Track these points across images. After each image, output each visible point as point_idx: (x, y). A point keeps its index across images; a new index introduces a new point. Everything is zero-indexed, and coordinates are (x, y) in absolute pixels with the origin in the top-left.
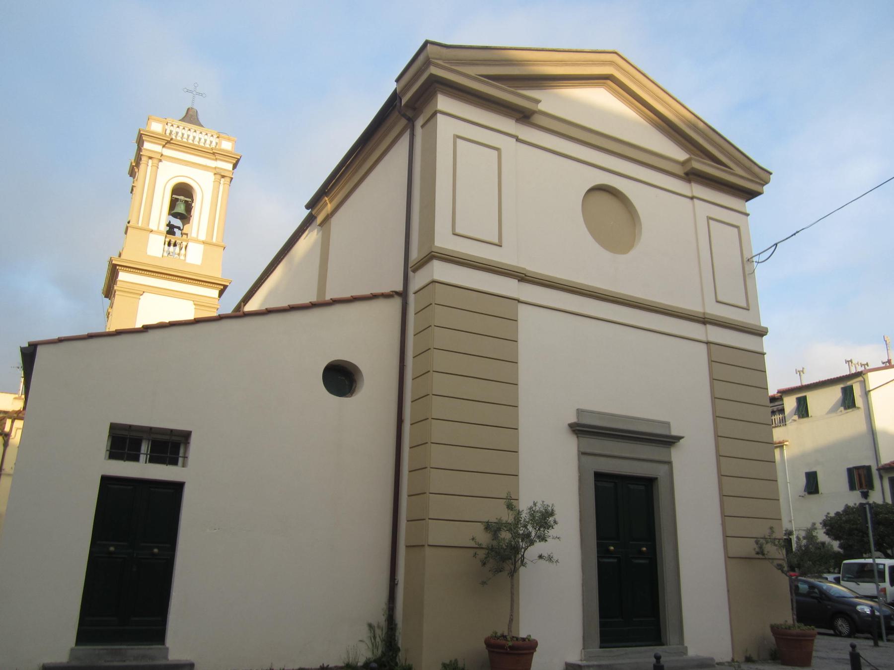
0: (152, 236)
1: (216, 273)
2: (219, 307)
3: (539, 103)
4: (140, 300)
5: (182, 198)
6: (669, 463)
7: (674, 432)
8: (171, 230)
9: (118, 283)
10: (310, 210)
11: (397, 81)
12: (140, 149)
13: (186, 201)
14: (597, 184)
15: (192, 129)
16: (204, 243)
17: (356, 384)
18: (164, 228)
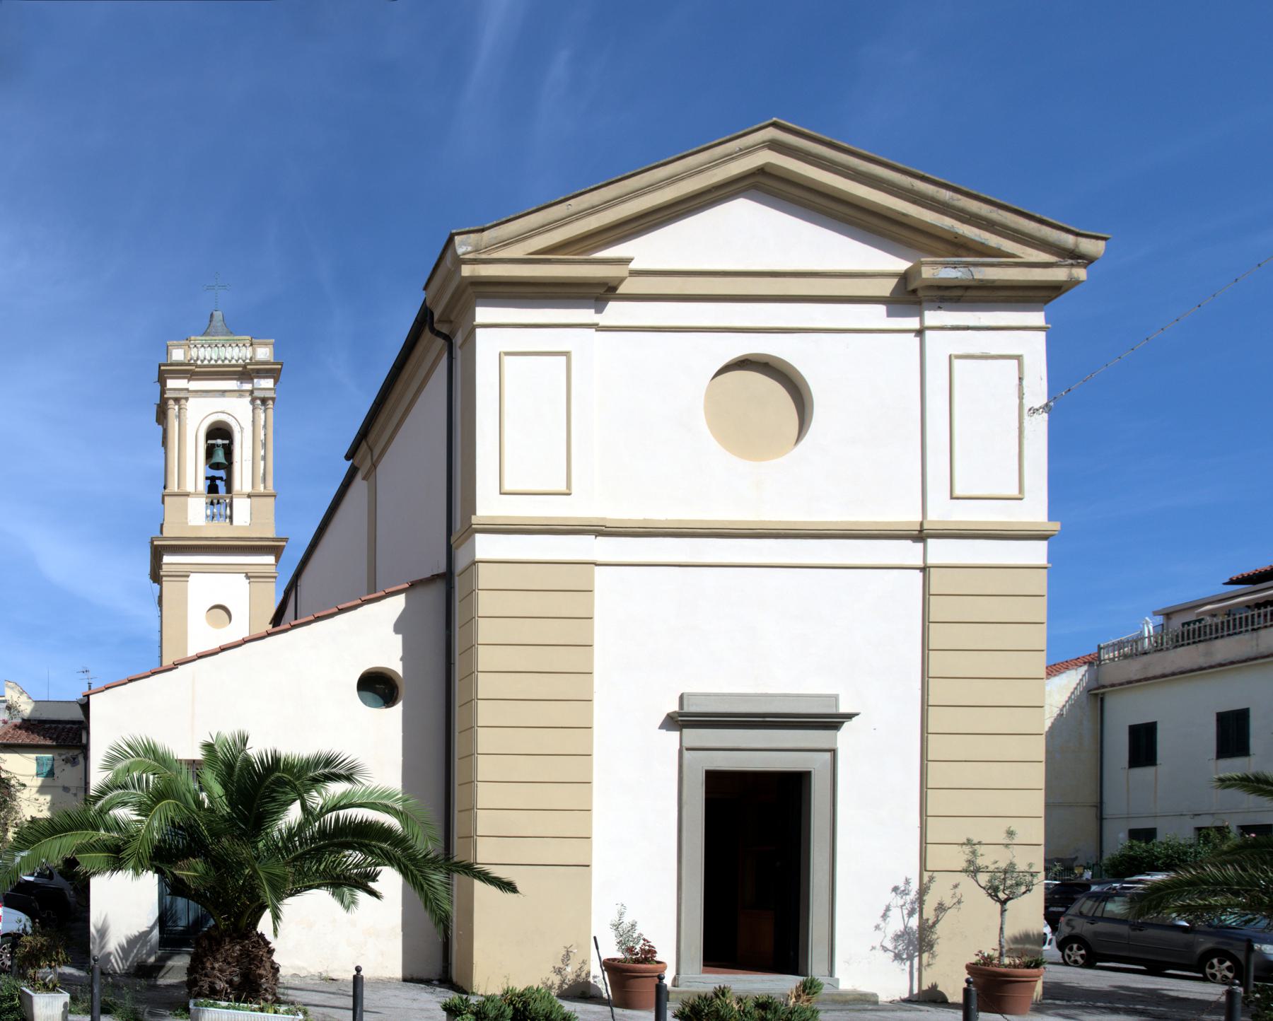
0: (190, 500)
1: (268, 531)
2: (276, 575)
3: (630, 262)
4: (189, 583)
5: (219, 442)
6: (833, 752)
7: (843, 709)
8: (212, 489)
9: (164, 566)
10: (351, 461)
11: (425, 288)
12: (163, 392)
13: (223, 444)
14: (371, 667)
15: (219, 343)
16: (249, 496)
17: (398, 691)
18: (202, 485)
